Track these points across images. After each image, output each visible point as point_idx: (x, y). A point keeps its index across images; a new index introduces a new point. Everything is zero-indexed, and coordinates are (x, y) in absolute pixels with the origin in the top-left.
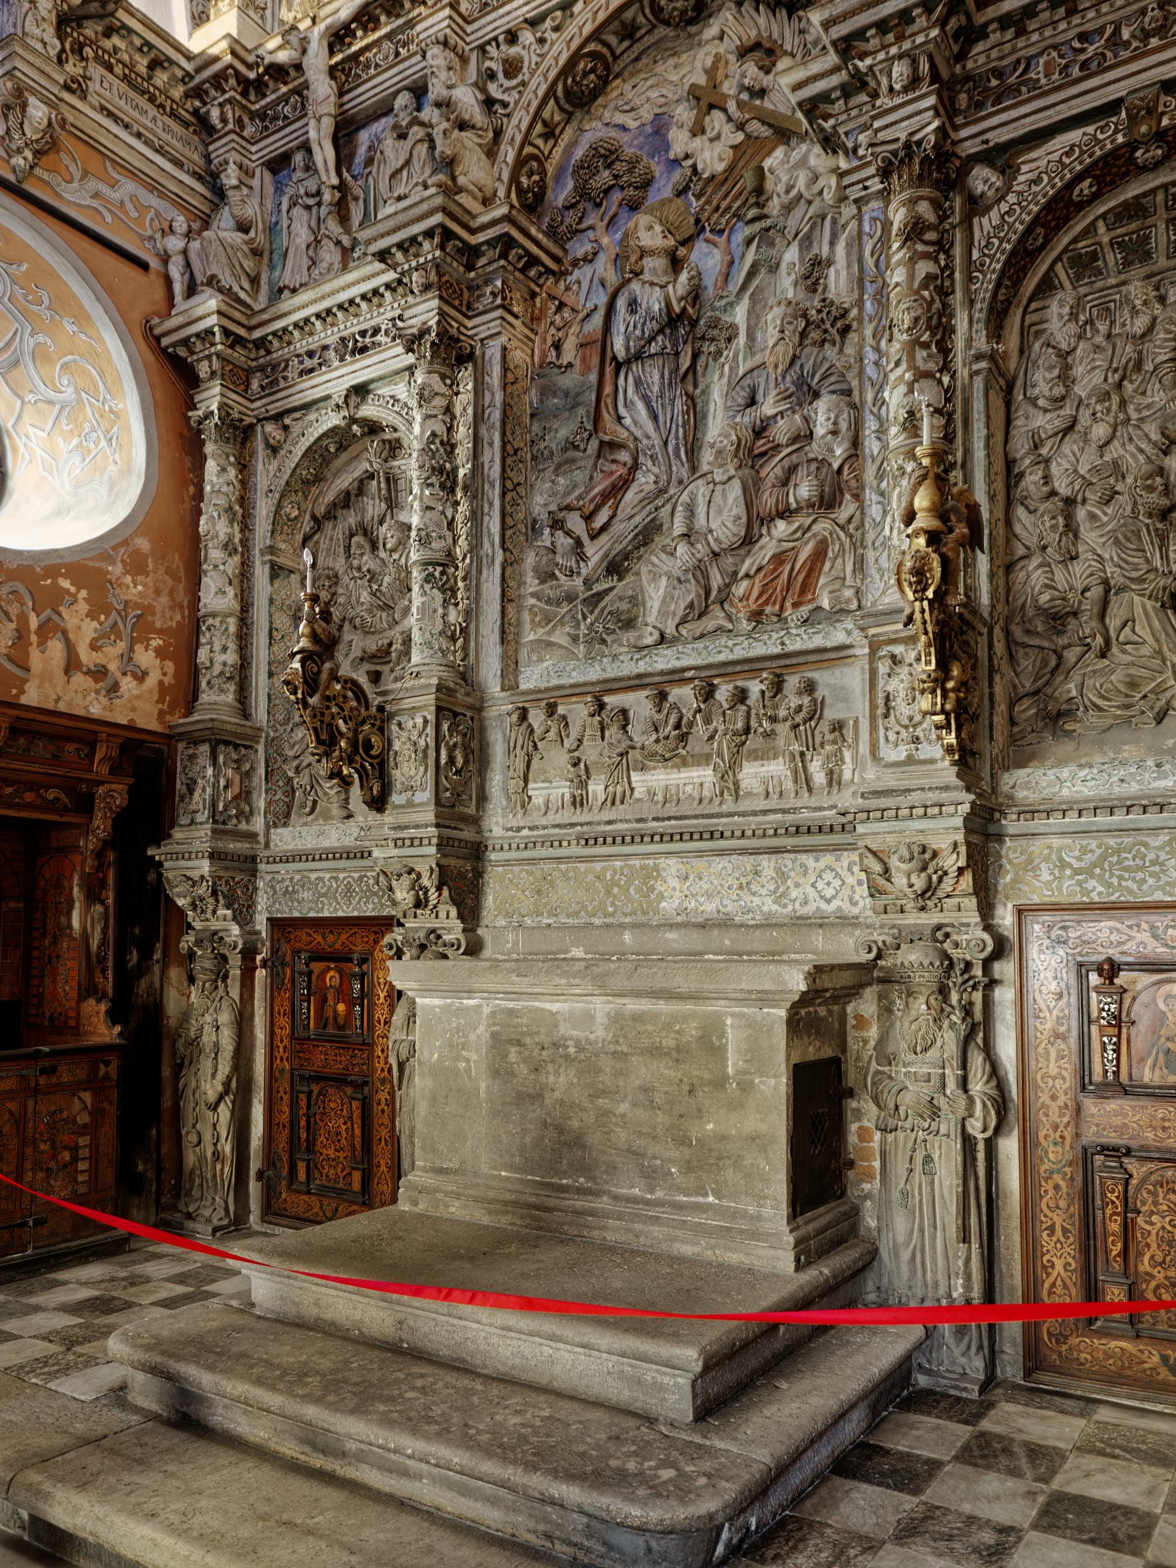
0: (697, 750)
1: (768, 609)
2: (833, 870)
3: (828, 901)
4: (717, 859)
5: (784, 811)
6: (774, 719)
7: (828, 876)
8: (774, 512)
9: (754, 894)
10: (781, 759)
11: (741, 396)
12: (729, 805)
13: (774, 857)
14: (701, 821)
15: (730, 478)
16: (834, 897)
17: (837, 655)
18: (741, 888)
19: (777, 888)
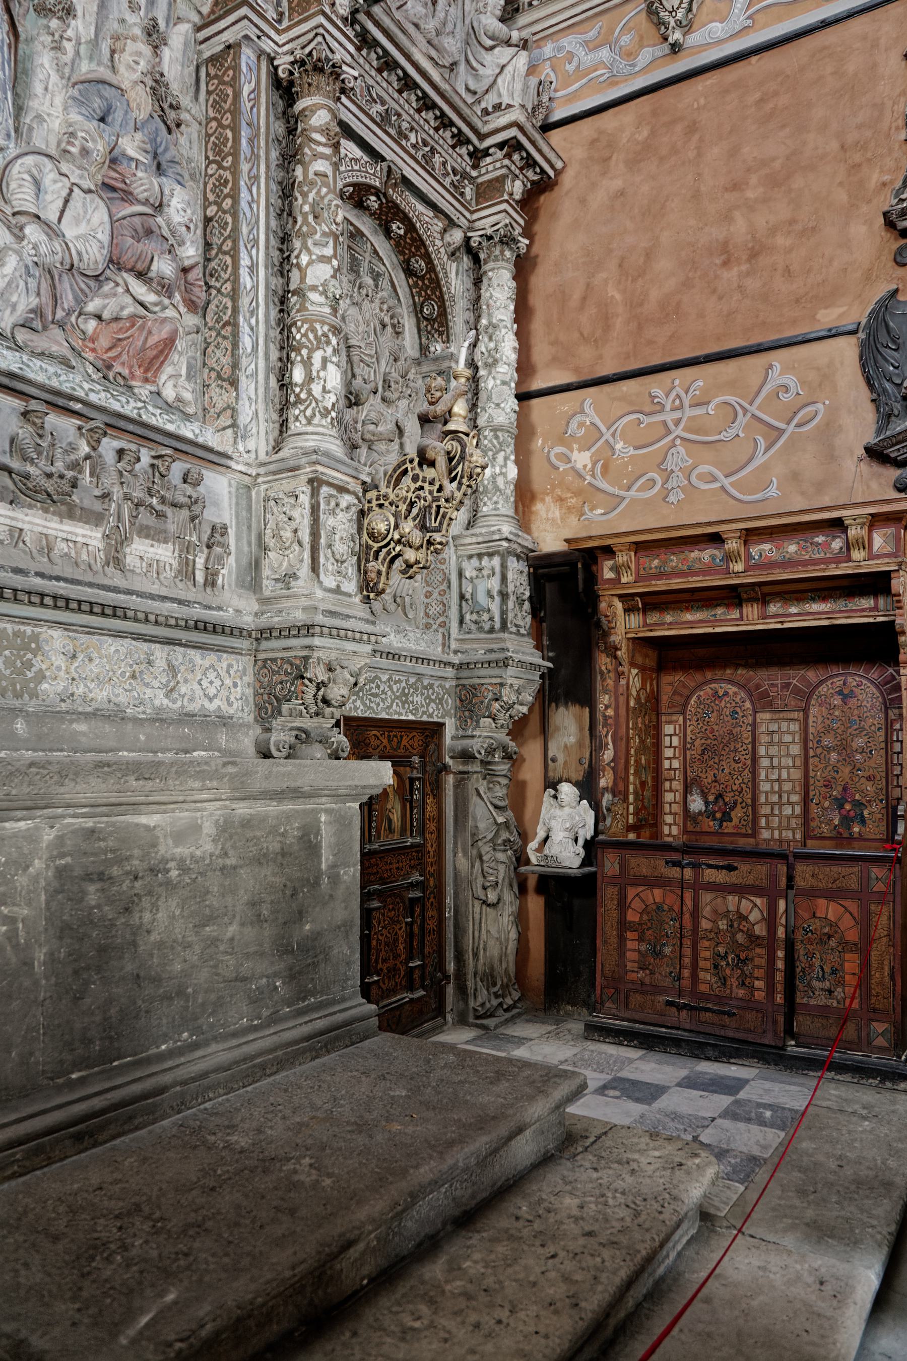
0: (87, 503)
1: (117, 368)
2: (215, 670)
3: (211, 700)
4: (110, 640)
5: (180, 602)
6: (163, 500)
7: (212, 675)
8: (129, 267)
9: (147, 685)
10: (170, 546)
11: (97, 103)
12: (118, 581)
13: (166, 647)
14: (96, 591)
15: (90, 191)
16: (215, 696)
17: (216, 459)
18: (133, 676)
19: (169, 681)
